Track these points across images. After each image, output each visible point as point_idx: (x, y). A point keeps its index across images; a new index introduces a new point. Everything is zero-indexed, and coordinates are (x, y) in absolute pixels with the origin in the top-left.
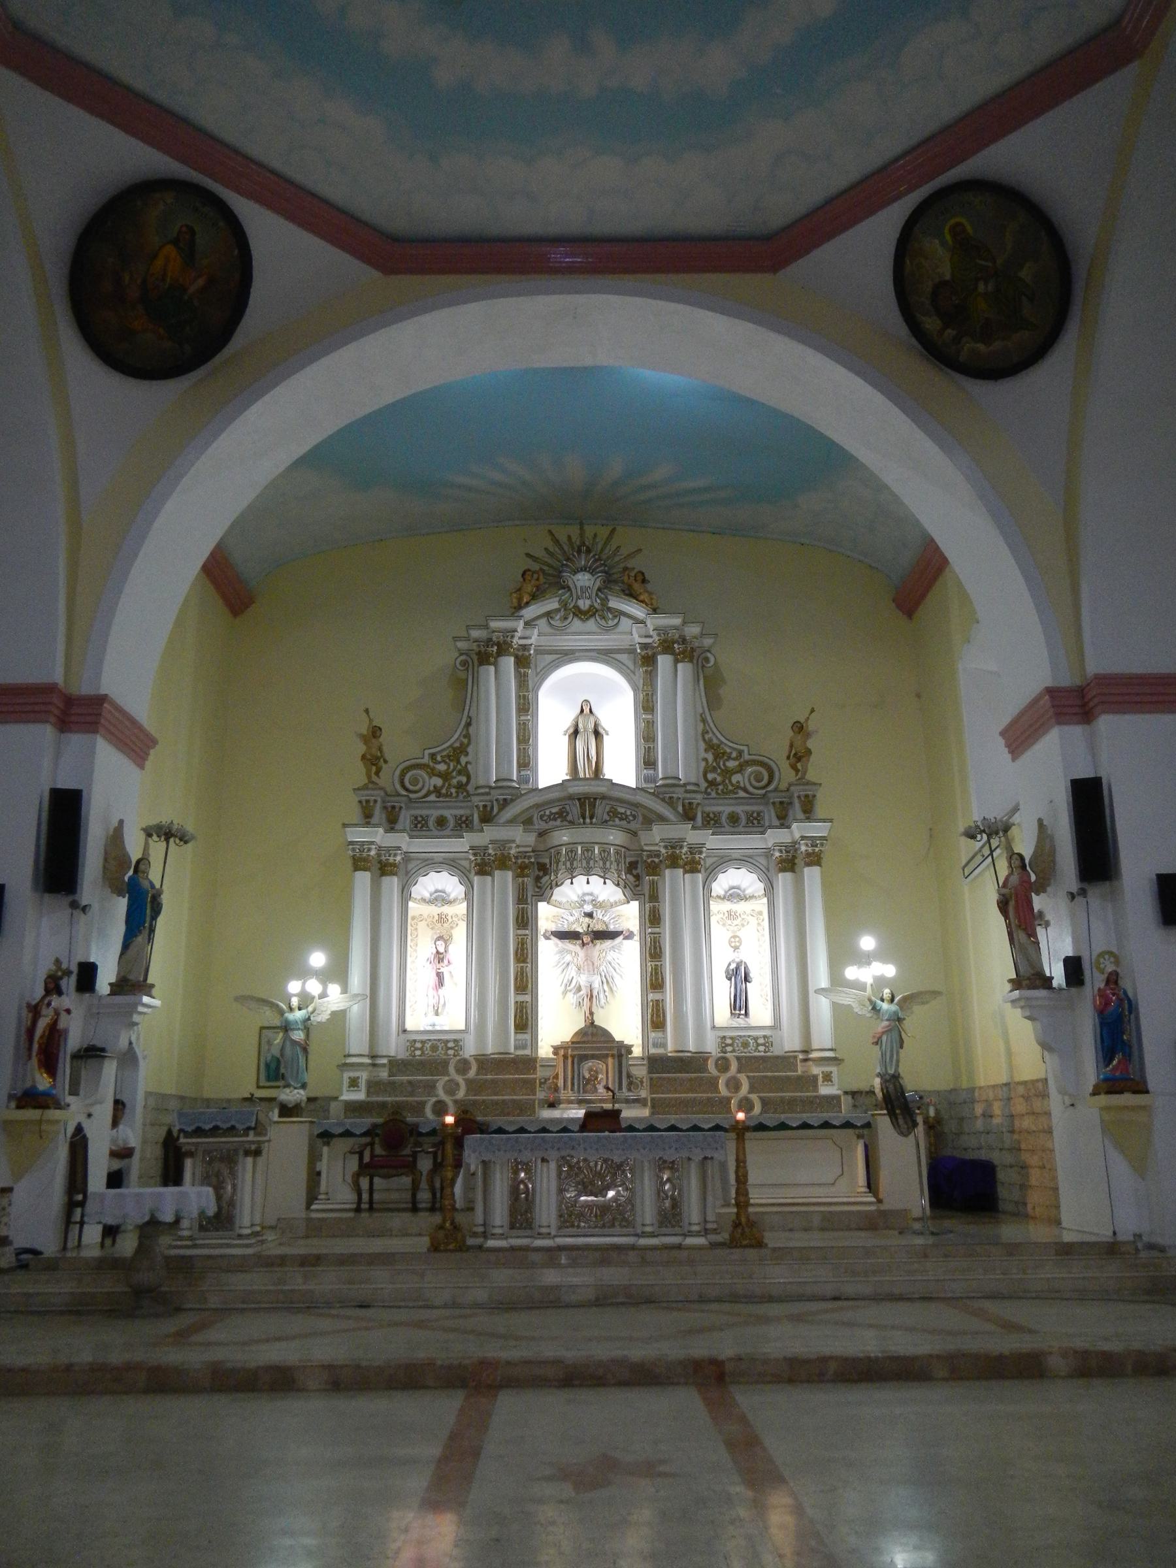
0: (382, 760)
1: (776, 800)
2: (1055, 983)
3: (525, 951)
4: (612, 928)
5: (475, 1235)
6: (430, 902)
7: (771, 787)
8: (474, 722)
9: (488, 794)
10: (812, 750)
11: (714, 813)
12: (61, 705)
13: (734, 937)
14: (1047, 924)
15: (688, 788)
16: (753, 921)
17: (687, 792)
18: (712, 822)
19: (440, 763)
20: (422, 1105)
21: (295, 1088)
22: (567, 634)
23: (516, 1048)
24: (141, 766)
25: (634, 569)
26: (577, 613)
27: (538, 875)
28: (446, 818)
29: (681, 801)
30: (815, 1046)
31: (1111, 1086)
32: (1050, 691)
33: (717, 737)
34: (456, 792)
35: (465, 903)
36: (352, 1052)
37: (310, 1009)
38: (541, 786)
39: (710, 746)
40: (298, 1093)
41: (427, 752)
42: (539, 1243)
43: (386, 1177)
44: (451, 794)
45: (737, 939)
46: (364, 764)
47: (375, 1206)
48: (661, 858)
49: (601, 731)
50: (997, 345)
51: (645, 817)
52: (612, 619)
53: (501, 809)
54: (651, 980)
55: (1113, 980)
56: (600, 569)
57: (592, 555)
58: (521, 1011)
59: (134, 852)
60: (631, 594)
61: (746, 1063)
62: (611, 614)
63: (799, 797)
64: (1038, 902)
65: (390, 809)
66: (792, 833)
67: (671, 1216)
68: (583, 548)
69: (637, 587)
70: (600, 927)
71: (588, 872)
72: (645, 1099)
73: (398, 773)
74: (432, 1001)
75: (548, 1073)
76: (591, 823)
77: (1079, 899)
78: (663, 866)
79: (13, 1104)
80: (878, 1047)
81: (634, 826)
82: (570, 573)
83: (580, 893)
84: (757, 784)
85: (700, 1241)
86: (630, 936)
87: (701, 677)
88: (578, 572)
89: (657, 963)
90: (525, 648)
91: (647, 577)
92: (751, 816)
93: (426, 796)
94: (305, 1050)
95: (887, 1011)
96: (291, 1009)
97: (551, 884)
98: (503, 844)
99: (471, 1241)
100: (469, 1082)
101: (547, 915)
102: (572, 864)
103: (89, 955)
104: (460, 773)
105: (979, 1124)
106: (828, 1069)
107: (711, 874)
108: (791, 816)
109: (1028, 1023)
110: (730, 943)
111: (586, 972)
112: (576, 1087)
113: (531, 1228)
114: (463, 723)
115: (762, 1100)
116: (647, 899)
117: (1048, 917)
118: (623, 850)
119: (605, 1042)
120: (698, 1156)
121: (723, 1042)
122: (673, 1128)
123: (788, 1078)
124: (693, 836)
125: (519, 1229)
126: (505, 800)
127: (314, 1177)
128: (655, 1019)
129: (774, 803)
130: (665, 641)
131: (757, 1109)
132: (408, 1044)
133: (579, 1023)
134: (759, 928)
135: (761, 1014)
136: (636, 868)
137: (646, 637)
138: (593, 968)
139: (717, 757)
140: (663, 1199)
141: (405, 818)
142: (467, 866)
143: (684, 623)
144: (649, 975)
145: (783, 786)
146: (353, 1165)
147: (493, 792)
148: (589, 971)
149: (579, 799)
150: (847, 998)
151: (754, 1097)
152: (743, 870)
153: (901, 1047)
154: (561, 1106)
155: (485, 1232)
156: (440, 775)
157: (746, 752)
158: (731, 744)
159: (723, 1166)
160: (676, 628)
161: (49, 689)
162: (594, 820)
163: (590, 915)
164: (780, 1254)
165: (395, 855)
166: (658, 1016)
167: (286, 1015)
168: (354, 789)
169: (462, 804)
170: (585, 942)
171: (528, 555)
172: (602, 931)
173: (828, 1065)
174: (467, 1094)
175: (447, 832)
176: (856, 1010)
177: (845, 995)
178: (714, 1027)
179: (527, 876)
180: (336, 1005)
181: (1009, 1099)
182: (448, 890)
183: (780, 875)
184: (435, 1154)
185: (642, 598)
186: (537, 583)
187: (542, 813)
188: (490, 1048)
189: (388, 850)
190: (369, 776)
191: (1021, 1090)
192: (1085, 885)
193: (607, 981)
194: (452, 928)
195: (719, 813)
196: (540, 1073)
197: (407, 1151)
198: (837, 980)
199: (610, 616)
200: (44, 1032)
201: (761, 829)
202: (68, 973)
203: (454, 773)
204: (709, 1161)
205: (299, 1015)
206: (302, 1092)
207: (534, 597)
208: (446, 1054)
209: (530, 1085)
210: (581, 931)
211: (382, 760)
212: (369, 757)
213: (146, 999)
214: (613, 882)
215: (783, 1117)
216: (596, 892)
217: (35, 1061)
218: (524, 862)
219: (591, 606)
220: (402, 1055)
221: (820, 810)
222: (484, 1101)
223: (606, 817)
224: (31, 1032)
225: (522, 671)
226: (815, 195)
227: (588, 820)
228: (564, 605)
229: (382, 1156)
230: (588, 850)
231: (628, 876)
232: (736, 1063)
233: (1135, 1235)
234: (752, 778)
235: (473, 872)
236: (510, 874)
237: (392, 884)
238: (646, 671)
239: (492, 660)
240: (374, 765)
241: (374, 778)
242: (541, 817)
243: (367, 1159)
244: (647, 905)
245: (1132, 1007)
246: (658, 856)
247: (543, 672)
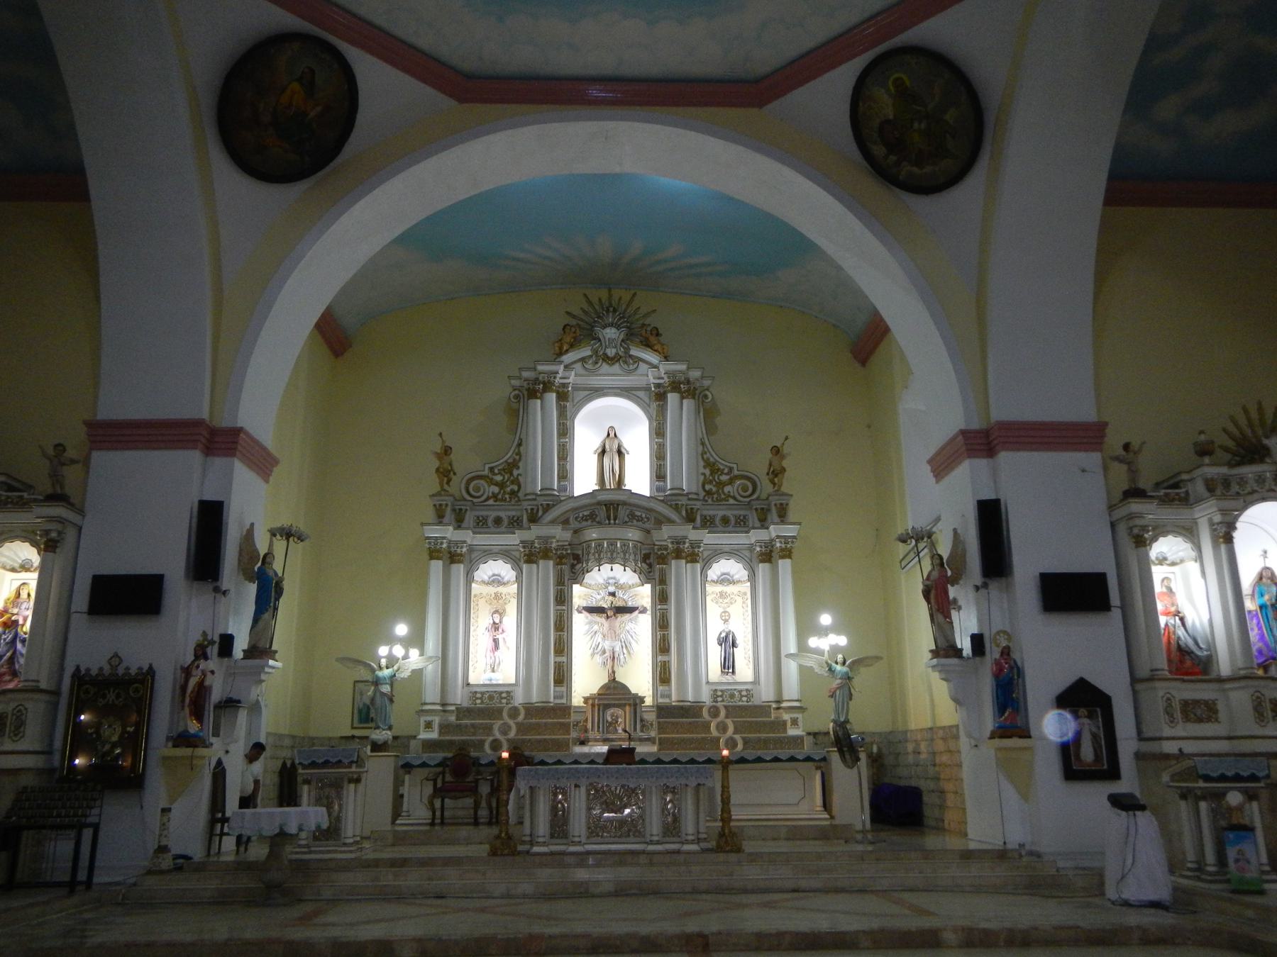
0: (452, 473)
1: (758, 506)
2: (965, 653)
4: (630, 604)
5: (523, 843)
6: (488, 584)
7: (755, 497)
8: (524, 443)
9: (535, 500)
10: (787, 469)
11: (710, 516)
12: (207, 436)
13: (725, 612)
14: (959, 608)
15: (690, 496)
16: (739, 600)
17: (689, 499)
18: (708, 523)
19: (496, 474)
20: (482, 743)
21: (384, 730)
22: (597, 375)
23: (554, 698)
24: (267, 481)
25: (649, 325)
26: (606, 359)
28: (501, 518)
29: (684, 507)
30: (786, 697)
31: (1003, 732)
32: (964, 433)
33: (713, 457)
34: (510, 498)
35: (516, 585)
36: (428, 701)
37: (395, 668)
38: (575, 495)
39: (708, 464)
40: (386, 734)
41: (487, 466)
42: (572, 849)
43: (456, 798)
44: (506, 498)
45: (727, 614)
46: (439, 477)
47: (446, 821)
49: (623, 450)
50: (928, 169)
51: (655, 518)
52: (633, 364)
53: (543, 514)
54: (660, 645)
55: (1006, 652)
56: (622, 326)
57: (617, 314)
58: (559, 669)
59: (262, 548)
61: (732, 711)
62: (632, 359)
63: (775, 505)
64: (953, 592)
65: (458, 511)
66: (770, 533)
67: (672, 828)
68: (611, 308)
69: (653, 339)
70: (620, 604)
71: (612, 561)
72: (654, 738)
73: (464, 481)
74: (490, 661)
75: (580, 717)
76: (615, 524)
77: (983, 591)
78: (669, 557)
79: (170, 744)
80: (833, 699)
81: (647, 526)
82: (601, 328)
83: (606, 577)
84: (745, 494)
85: (694, 847)
86: (644, 611)
87: (702, 410)
88: (607, 327)
90: (564, 385)
91: (661, 332)
92: (739, 518)
93: (486, 500)
94: (391, 701)
95: (840, 671)
96: (381, 668)
97: (583, 570)
98: (546, 540)
99: (520, 848)
100: (519, 725)
101: (580, 595)
102: (599, 555)
103: (227, 627)
104: (512, 483)
105: (911, 758)
106: (795, 715)
107: (707, 564)
108: (769, 520)
109: (945, 683)
110: (721, 616)
111: (610, 639)
112: (601, 729)
113: (567, 838)
114: (516, 443)
115: (744, 739)
116: (657, 582)
117: (960, 603)
118: (639, 544)
119: (623, 694)
120: (693, 783)
121: (715, 695)
122: (675, 761)
123: (764, 723)
124: (693, 535)
125: (557, 838)
126: (548, 505)
127: (398, 798)
128: (662, 675)
129: (756, 509)
130: (673, 382)
131: (740, 746)
132: (471, 695)
134: (744, 605)
135: (744, 671)
136: (649, 558)
137: (659, 378)
138: (614, 635)
139: (712, 473)
140: (667, 815)
141: (470, 518)
142: (518, 556)
143: (688, 368)
144: (658, 641)
145: (764, 496)
146: (429, 789)
147: (538, 498)
148: (612, 638)
149: (605, 505)
150: (810, 662)
151: (737, 737)
152: (732, 561)
153: (851, 699)
154: (590, 743)
155: (531, 841)
156: (496, 484)
157: (735, 469)
158: (723, 462)
159: (712, 790)
160: (680, 372)
161: (198, 423)
162: (617, 521)
163: (613, 594)
164: (754, 858)
165: (462, 547)
166: (665, 673)
167: (377, 672)
168: (430, 496)
169: (511, 507)
170: (609, 615)
171: (568, 313)
173: (795, 713)
174: (515, 735)
175: (503, 529)
176: (816, 671)
177: (808, 659)
178: (708, 683)
179: (565, 564)
180: (415, 665)
181: (932, 740)
182: (503, 574)
183: (760, 565)
184: (492, 781)
185: (656, 348)
186: (574, 335)
187: (577, 515)
188: (535, 698)
189: (457, 543)
190: (441, 484)
191: (941, 733)
192: (987, 580)
193: (626, 646)
194: (505, 604)
195: (714, 516)
196: (574, 717)
197: (470, 779)
198: (802, 647)
199: (631, 362)
200: (194, 688)
201: (746, 529)
202: (212, 642)
203: (508, 483)
204: (702, 787)
205: (386, 673)
206: (389, 733)
207: (572, 346)
208: (501, 703)
209: (565, 728)
210: (606, 607)
211: (452, 473)
212: (441, 470)
213: (271, 662)
214: (632, 570)
215: (760, 753)
216: (618, 576)
217: (187, 710)
219: (617, 354)
220: (465, 704)
221: (792, 515)
222: (530, 740)
223: (627, 519)
224: (184, 688)
225: (562, 403)
226: (792, 51)
227: (612, 522)
228: (595, 352)
229: (451, 782)
230: (612, 545)
231: (643, 564)
232: (724, 711)
233: (1020, 845)
234: (740, 487)
235: (522, 561)
236: (551, 563)
237: (459, 569)
238: (659, 404)
239: (539, 395)
240: (446, 476)
241: (446, 487)
242: (576, 518)
243: (439, 784)
244: (657, 588)
245: (1020, 672)
247: (578, 405)
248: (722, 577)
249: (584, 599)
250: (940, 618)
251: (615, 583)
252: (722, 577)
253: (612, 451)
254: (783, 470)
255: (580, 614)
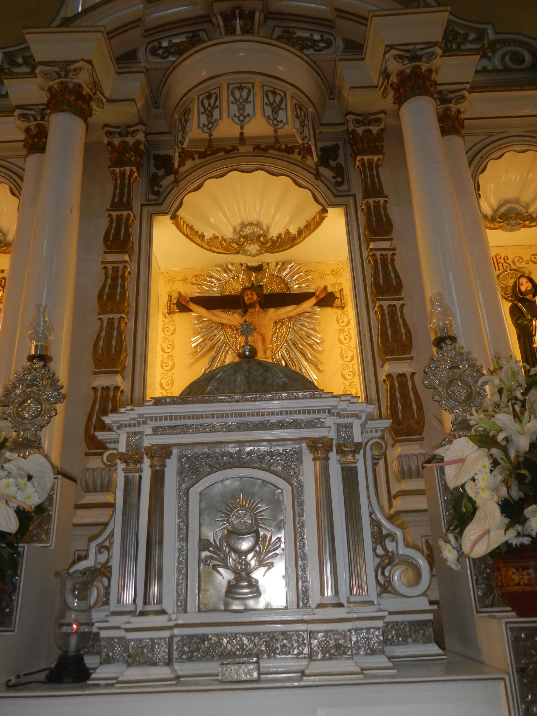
3: (119, 289)
4: (295, 288)
19: (19, 65)
27: (155, 175)
48: (382, 126)
54: (383, 334)
83: (237, 222)
89: (392, 303)
102: (210, 116)
118: (311, 110)
172: (278, 294)
179: (128, 163)
187: (156, 44)
218: (124, 142)
230: (241, 88)
242: (154, 52)
244: (359, 210)
246: (378, 121)
248: (505, 208)
249: (193, 284)
251: (259, 236)
252: (502, 210)
255: (184, 315)
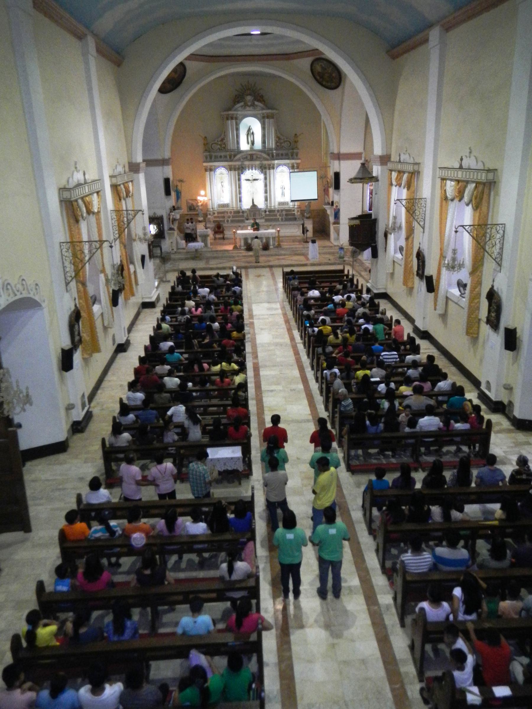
4: (257, 178)
33: (279, 135)
50: (329, 84)
55: (337, 206)
60: (258, 101)
98: (235, 166)
101: (243, 177)
128: (266, 200)
133: (251, 204)
217: (171, 223)
245: (339, 210)
250: (326, 196)
253: (250, 133)
254: (298, 141)
